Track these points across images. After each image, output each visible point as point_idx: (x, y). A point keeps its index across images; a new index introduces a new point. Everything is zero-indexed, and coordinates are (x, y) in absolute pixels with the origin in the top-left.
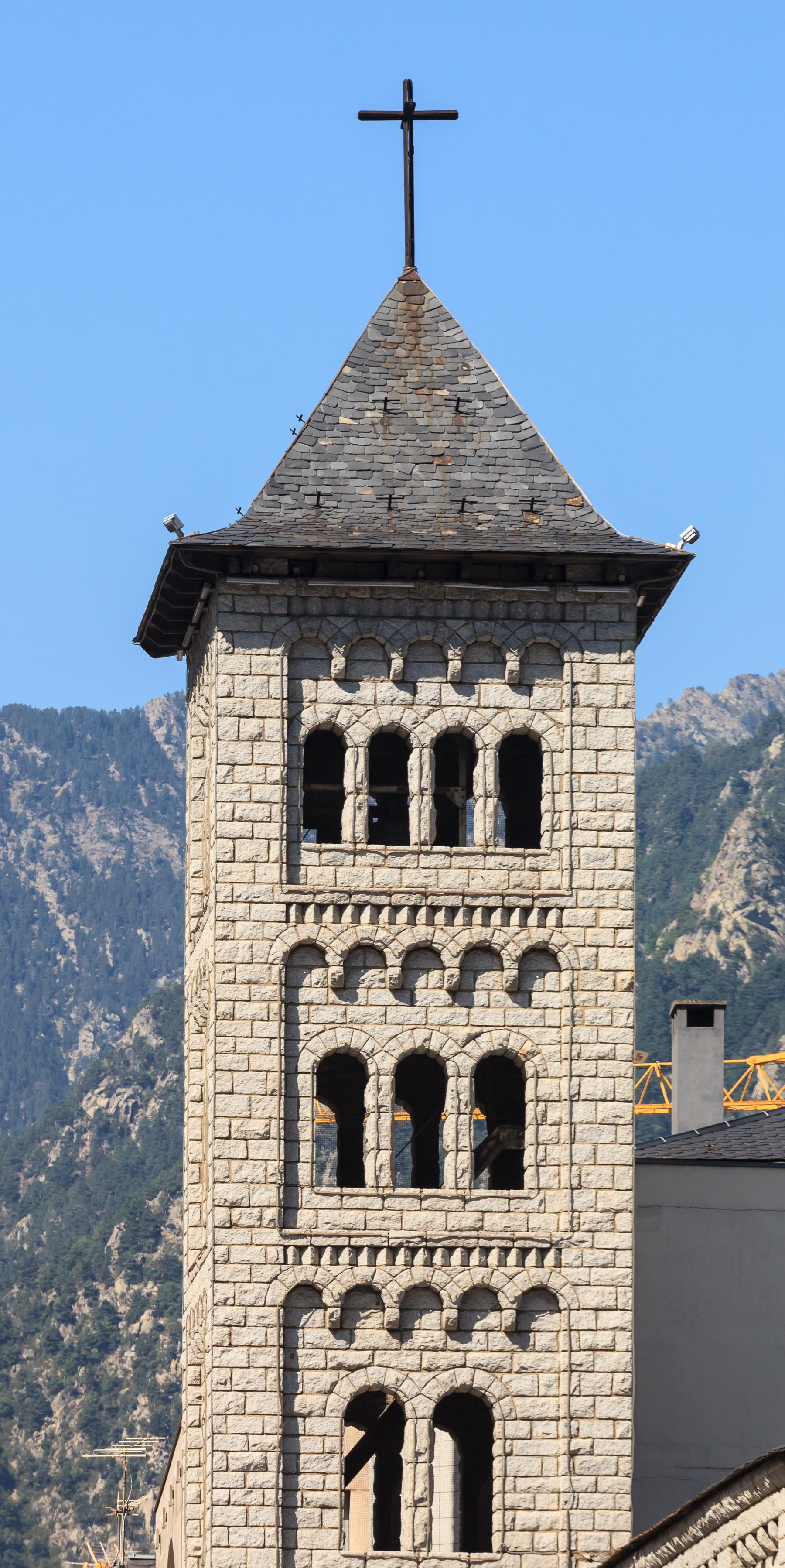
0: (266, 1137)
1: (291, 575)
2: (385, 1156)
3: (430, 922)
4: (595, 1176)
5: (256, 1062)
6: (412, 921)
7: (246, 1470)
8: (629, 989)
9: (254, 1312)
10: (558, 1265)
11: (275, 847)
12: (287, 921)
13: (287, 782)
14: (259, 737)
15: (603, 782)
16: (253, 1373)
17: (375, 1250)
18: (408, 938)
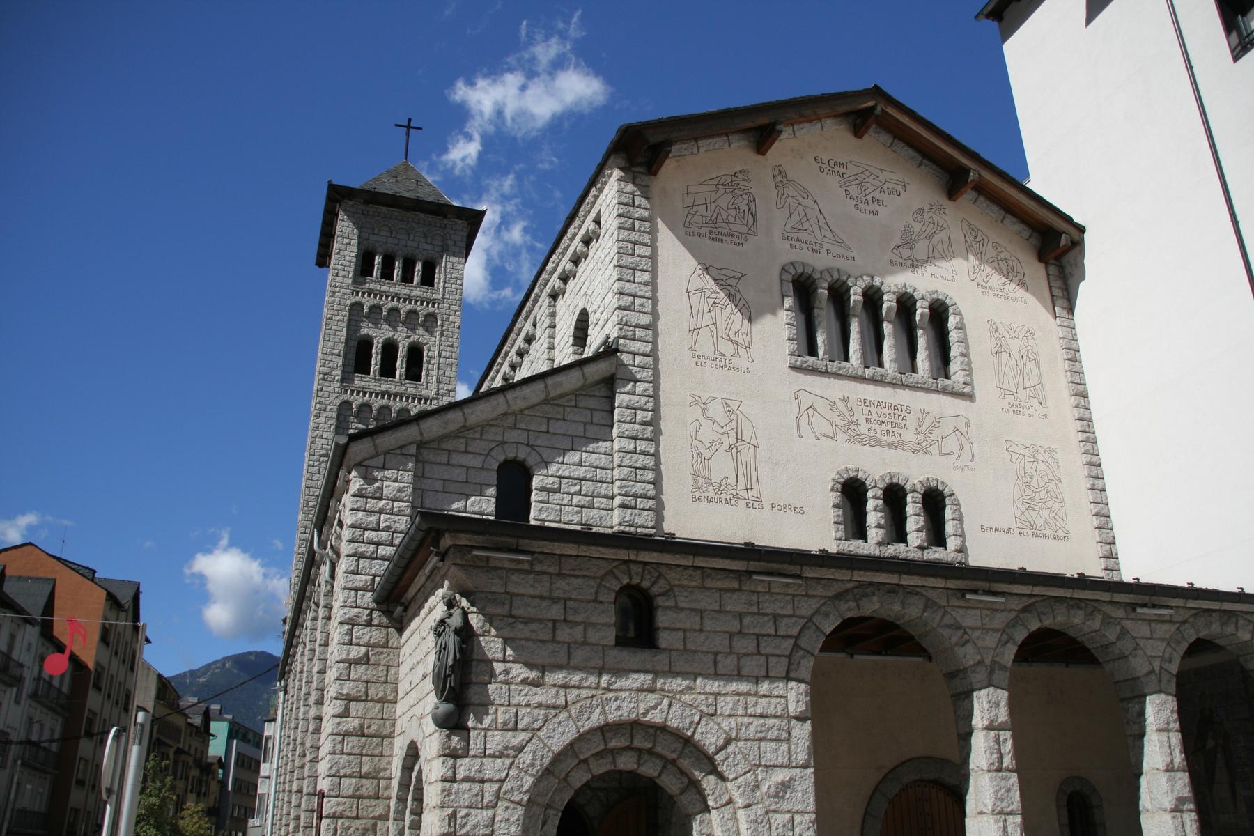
0: (339, 355)
1: (364, 203)
2: (378, 367)
3: (398, 301)
4: (443, 379)
5: (337, 333)
6: (392, 300)
7: (321, 456)
8: (459, 328)
9: (329, 407)
10: (431, 404)
11: (351, 275)
12: (353, 294)
13: (357, 256)
14: (350, 244)
15: (455, 271)
16: (326, 426)
17: (371, 394)
18: (390, 305)
